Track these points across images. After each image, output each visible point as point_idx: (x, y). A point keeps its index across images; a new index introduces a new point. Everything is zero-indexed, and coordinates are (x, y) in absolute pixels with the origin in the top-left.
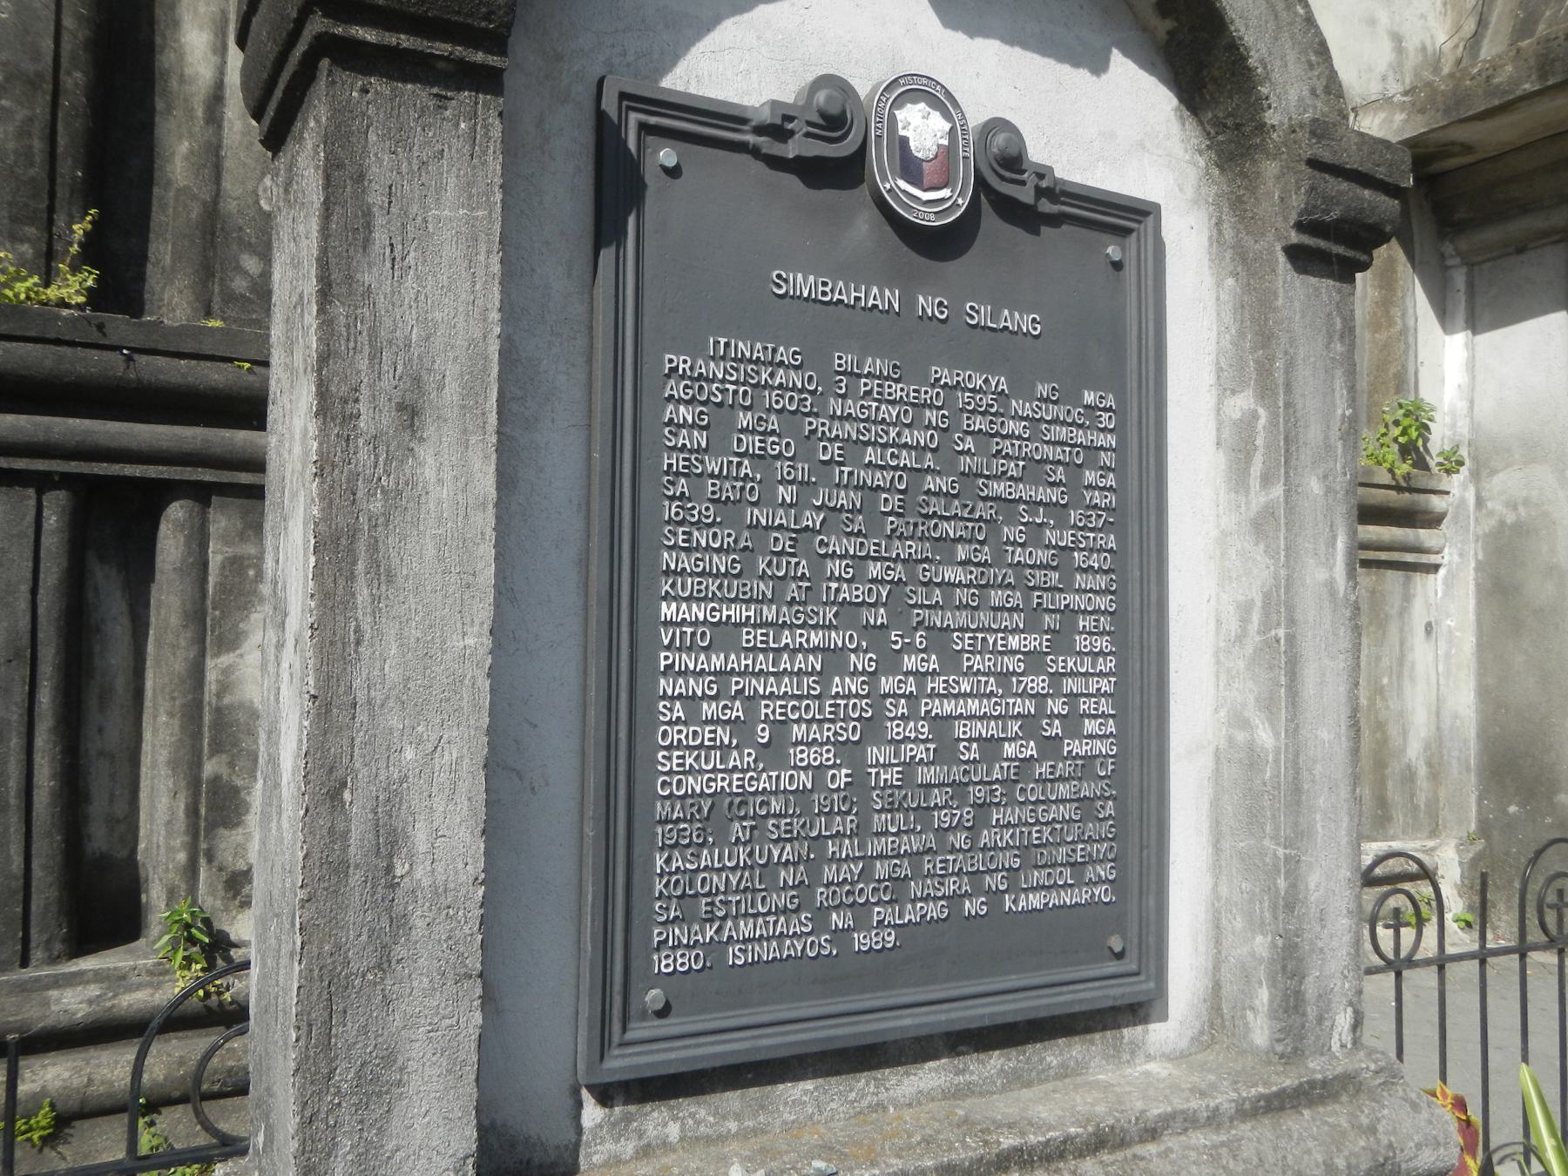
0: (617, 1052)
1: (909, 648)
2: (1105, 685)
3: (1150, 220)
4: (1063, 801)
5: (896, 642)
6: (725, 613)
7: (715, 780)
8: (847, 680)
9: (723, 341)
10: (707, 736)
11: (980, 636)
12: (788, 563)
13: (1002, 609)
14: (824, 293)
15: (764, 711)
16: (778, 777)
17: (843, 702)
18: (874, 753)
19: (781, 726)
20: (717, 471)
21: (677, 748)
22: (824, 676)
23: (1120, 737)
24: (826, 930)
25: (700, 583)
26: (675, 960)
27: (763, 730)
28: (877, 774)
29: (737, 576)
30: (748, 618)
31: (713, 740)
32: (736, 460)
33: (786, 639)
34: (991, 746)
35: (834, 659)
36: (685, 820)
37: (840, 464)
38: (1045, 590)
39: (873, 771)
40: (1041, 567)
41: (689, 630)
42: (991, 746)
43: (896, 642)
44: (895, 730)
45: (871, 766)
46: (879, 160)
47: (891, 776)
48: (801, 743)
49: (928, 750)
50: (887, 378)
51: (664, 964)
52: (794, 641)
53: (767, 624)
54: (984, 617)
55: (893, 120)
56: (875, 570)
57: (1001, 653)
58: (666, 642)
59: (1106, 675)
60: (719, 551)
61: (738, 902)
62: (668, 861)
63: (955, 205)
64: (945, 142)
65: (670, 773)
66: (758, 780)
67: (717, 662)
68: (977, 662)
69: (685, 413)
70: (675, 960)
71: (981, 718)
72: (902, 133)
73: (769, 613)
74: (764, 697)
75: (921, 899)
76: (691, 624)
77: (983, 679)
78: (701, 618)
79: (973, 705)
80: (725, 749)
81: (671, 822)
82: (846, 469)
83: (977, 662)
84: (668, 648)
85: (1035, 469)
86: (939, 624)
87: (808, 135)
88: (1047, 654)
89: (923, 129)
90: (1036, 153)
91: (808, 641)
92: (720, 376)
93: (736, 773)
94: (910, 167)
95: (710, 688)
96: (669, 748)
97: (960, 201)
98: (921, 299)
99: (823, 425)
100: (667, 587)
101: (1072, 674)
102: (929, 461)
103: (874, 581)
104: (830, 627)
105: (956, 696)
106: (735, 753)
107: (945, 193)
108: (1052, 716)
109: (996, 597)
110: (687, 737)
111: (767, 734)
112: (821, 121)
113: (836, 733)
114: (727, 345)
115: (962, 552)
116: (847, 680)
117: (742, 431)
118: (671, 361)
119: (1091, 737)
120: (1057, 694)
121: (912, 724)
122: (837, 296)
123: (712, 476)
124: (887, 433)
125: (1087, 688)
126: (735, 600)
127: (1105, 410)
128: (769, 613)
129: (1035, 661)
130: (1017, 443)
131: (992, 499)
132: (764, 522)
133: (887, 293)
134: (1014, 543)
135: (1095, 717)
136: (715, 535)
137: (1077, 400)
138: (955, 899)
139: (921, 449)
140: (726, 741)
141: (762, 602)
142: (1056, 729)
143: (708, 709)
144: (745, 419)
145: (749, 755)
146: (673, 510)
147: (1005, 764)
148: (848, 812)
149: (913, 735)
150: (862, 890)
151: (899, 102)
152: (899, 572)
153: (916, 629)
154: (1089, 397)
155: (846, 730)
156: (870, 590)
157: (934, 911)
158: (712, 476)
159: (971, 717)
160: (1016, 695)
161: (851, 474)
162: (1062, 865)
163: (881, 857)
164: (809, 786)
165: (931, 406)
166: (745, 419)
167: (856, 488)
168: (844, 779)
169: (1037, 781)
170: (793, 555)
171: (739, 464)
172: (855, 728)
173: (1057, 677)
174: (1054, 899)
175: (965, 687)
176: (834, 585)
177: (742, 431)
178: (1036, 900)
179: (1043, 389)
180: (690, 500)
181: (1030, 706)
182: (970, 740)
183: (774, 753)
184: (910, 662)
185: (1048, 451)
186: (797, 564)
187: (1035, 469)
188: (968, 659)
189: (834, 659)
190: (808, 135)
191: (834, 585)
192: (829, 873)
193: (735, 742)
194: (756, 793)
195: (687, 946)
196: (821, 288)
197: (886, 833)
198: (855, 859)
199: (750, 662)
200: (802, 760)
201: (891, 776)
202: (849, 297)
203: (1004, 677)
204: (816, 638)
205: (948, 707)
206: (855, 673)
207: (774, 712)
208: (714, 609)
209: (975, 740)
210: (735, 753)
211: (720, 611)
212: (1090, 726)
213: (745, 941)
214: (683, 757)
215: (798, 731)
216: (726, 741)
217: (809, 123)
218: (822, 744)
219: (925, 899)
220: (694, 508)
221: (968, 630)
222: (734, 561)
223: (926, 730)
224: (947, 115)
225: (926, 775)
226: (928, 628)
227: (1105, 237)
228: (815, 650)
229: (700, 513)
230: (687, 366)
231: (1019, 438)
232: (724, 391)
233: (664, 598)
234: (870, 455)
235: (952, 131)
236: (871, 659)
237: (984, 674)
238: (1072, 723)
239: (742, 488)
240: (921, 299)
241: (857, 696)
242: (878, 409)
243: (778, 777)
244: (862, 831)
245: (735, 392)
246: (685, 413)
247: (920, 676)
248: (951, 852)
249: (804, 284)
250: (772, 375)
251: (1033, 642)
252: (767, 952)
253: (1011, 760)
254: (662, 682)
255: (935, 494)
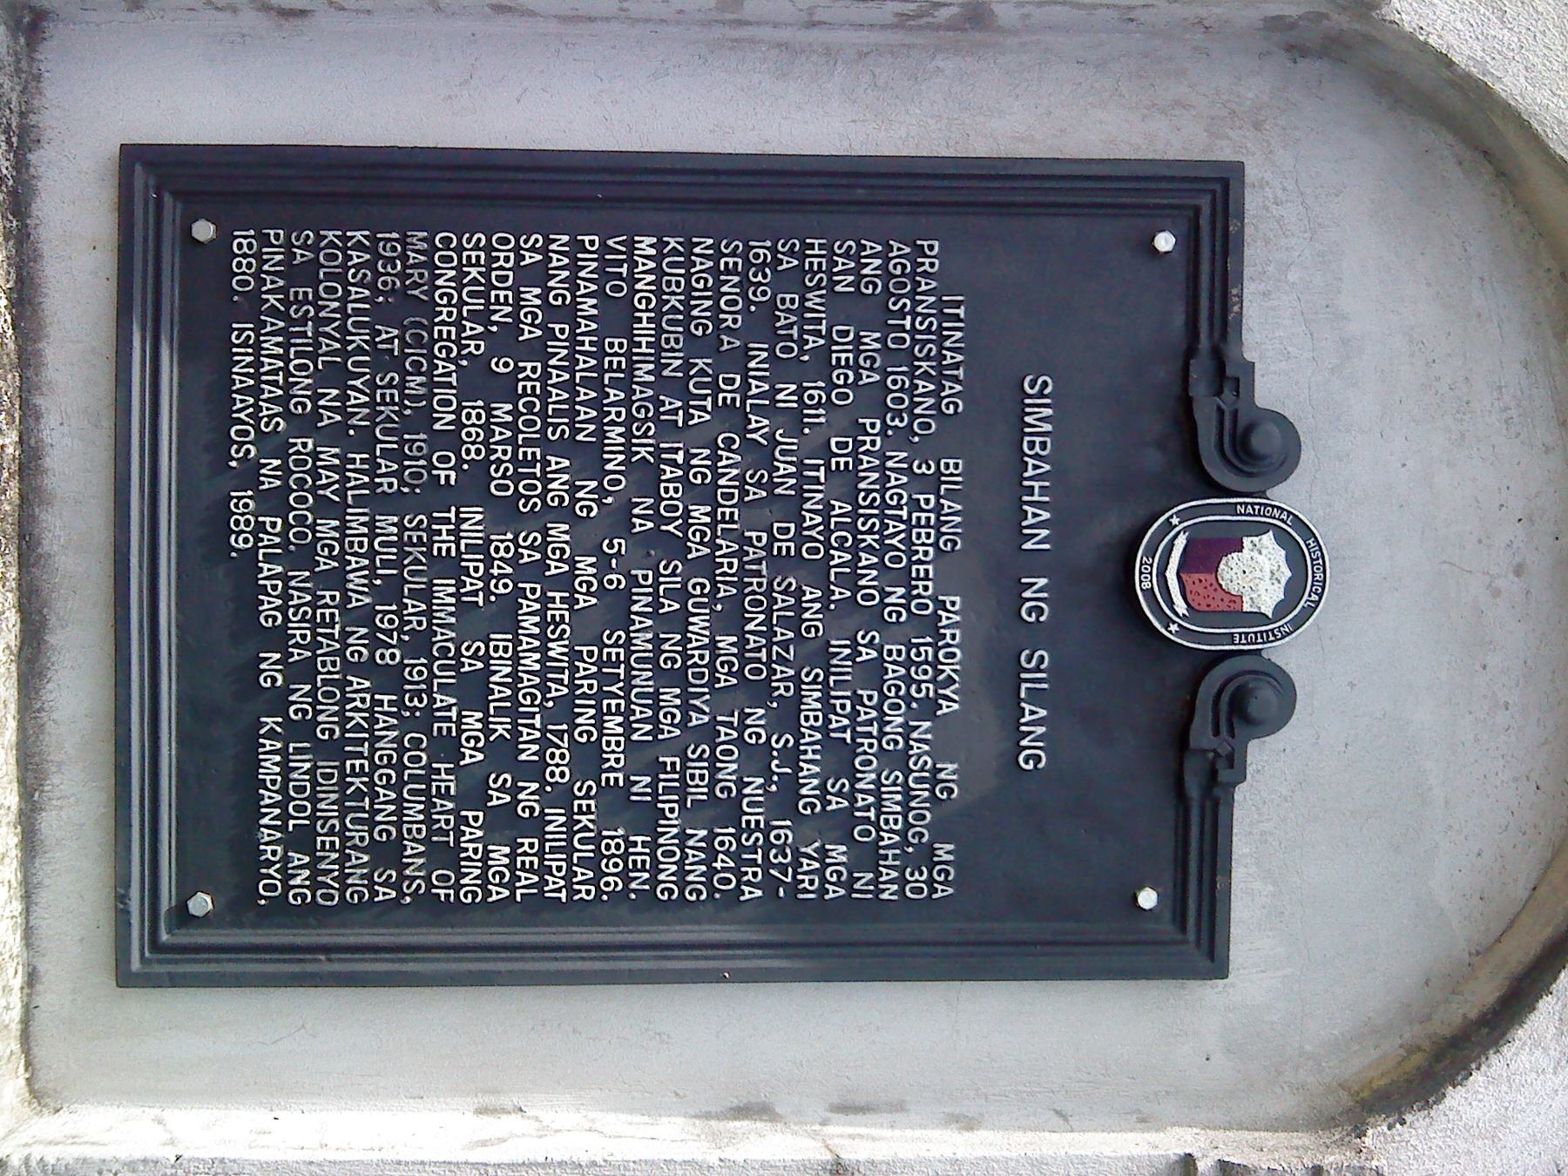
0: (152, 182)
1: (603, 566)
2: (554, 882)
3: (1205, 963)
4: (399, 812)
5: (611, 546)
6: (644, 316)
7: (449, 304)
8: (566, 477)
9: (961, 312)
10: (502, 293)
11: (621, 671)
12: (704, 397)
13: (656, 708)
14: (1032, 445)
15: (529, 365)
16: (449, 385)
17: (537, 470)
18: (475, 514)
19: (507, 388)
20: (809, 304)
21: (488, 255)
22: (568, 447)
23: (486, 910)
24: (259, 456)
25: (678, 284)
26: (245, 256)
27: (506, 365)
28: (447, 521)
29: (687, 331)
30: (639, 345)
31: (497, 302)
32: (823, 328)
33: (614, 394)
34: (474, 691)
35: (589, 459)
36: (405, 267)
37: (828, 466)
38: (682, 780)
39: (452, 515)
40: (714, 770)
41: (624, 270)
42: (474, 691)
43: (611, 546)
44: (502, 544)
45: (458, 513)
46: (1213, 512)
47: (444, 543)
48: (489, 416)
49: (475, 593)
50: (940, 534)
51: (243, 241)
52: (611, 404)
53: (631, 370)
54: (643, 678)
55: (1259, 529)
56: (700, 513)
57: (598, 707)
58: (610, 242)
59: (569, 886)
60: (716, 308)
61: (304, 335)
62: (359, 246)
63: (1167, 622)
64: (1247, 608)
65: (460, 249)
66: (447, 359)
67: (588, 306)
68: (586, 667)
69: (872, 266)
70: (245, 256)
71: (514, 674)
72: (1247, 541)
73: (644, 372)
74: (545, 366)
75: (286, 587)
76: (631, 272)
77: (566, 677)
78: (638, 286)
79: (531, 661)
80: (483, 317)
81: (404, 250)
82: (821, 474)
83: (586, 667)
84: (603, 244)
85: (841, 758)
86: (635, 608)
87: (1221, 411)
88: (598, 784)
89: (1257, 573)
90: (1261, 754)
91: (613, 423)
92: (919, 309)
93: (456, 335)
94: (1206, 553)
95: (555, 298)
96: (489, 248)
97: (1174, 628)
98: (1042, 582)
99: (873, 443)
100: (673, 244)
101: (571, 823)
102: (839, 593)
103: (687, 514)
104: (629, 453)
105: (544, 638)
106: (480, 329)
107: (1181, 607)
108: (515, 791)
109: (671, 696)
110: (501, 268)
111: (502, 370)
112: (1240, 430)
113: (499, 462)
114: (957, 318)
115: (726, 641)
116: (566, 477)
117: (858, 338)
118: (931, 248)
119: (485, 858)
120: (546, 800)
121: (509, 570)
122: (1031, 462)
123: (803, 299)
124: (870, 532)
125: (553, 850)
126: (660, 330)
127: (931, 882)
128: (644, 372)
129: (589, 758)
130: (874, 730)
131: (798, 689)
132: (752, 365)
133: (1044, 533)
134: (742, 727)
135: (512, 866)
136: (735, 303)
137: (941, 832)
138: (279, 638)
139: (851, 580)
140: (495, 318)
141: (657, 362)
142: (499, 799)
143: (532, 294)
144: (871, 340)
145: (477, 347)
146: (761, 251)
147: (454, 714)
148: (402, 483)
149: (495, 572)
150: (304, 500)
151: (1283, 539)
152: (698, 552)
153: (628, 576)
154: (944, 851)
155: (504, 477)
156: (676, 508)
157: (269, 604)
158: (803, 299)
159: (516, 660)
160: (544, 731)
161: (817, 481)
162: (315, 810)
163: (343, 528)
164: (437, 426)
165: (908, 597)
166: (871, 340)
167: (799, 489)
168: (443, 474)
169: (428, 767)
170: (715, 402)
171: (818, 333)
172: (507, 488)
173: (564, 797)
174: (269, 797)
175: (556, 649)
176: (680, 457)
177: (858, 338)
178: (270, 768)
179: (949, 770)
180: (775, 271)
181: (528, 754)
182: (486, 659)
183: (480, 383)
184: (586, 565)
185: (866, 781)
186: (704, 409)
187: (841, 758)
188: (590, 654)
189: (589, 459)
190: (1221, 411)
191: (680, 457)
192: (329, 454)
193: (494, 329)
194: (431, 357)
195: (260, 270)
196: (1038, 439)
197: (372, 536)
198: (342, 493)
199: (587, 348)
200: (469, 416)
201: (444, 543)
202: (1030, 478)
203: (566, 710)
204: (615, 434)
205: (529, 623)
206: (574, 489)
207: (528, 378)
208: (649, 300)
209: (488, 665)
210: (480, 329)
211: (647, 310)
212: (500, 854)
213: (258, 343)
214: (478, 264)
215: (503, 410)
216: (495, 318)
217: (1235, 414)
218: (486, 443)
219: (286, 597)
220: (765, 276)
221: (629, 653)
222: (706, 327)
223: (502, 591)
224: (1282, 609)
225: (445, 591)
226: (628, 588)
227: (1168, 878)
228: (601, 434)
229: (760, 284)
230: (927, 267)
231: (882, 734)
232: (902, 314)
233: (660, 240)
234: (840, 507)
235: (1260, 618)
236: (590, 509)
237: (572, 678)
238: (505, 824)
239: (790, 338)
240: (1042, 582)
241: (546, 491)
242: (899, 519)
243: (449, 385)
244: (376, 502)
245: (902, 328)
246: (872, 266)
247: (566, 582)
248: (342, 631)
249: (1039, 418)
250: (926, 376)
251: (614, 757)
252: (241, 376)
253: (459, 723)
254: (565, 238)
255: (799, 601)
